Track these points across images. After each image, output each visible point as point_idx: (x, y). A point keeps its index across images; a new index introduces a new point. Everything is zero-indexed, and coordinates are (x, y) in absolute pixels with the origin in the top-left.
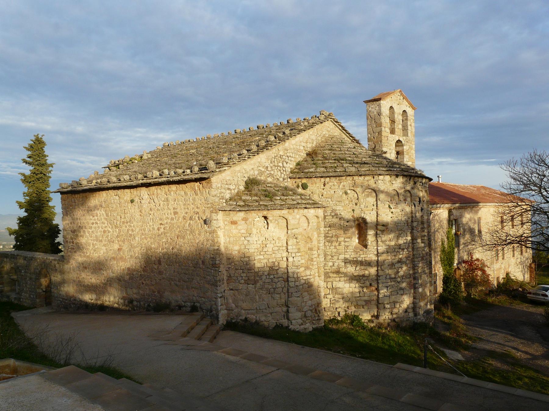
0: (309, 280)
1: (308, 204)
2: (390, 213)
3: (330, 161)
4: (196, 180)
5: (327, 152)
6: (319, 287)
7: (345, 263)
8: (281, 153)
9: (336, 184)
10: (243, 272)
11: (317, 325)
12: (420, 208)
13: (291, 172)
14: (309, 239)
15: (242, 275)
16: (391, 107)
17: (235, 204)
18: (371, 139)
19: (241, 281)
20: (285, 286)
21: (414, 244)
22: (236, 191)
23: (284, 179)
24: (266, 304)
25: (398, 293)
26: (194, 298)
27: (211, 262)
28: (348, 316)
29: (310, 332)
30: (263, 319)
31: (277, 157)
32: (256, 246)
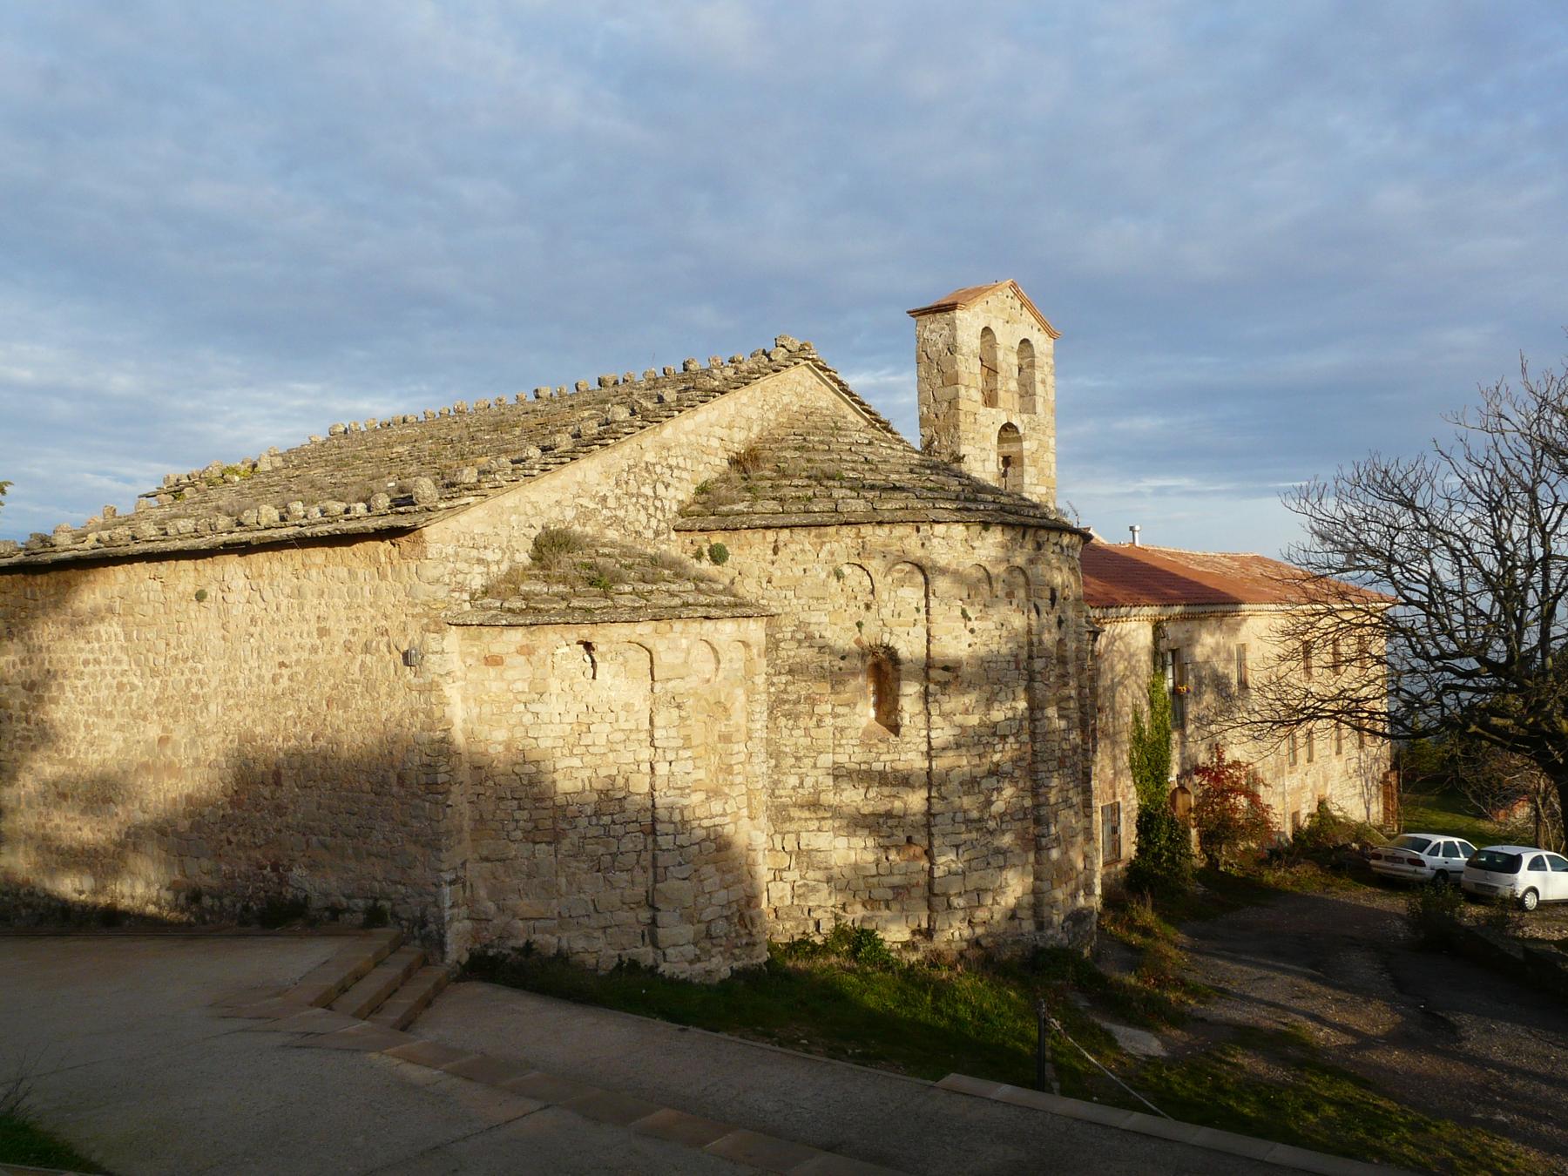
0: (719, 828)
1: (715, 606)
2: (967, 632)
3: (796, 482)
4: (380, 535)
5: (789, 454)
6: (750, 848)
7: (836, 777)
8: (650, 457)
9: (808, 547)
10: (520, 808)
11: (745, 962)
12: (1053, 619)
13: (682, 513)
14: (720, 710)
15: (517, 815)
16: (987, 330)
17: (499, 604)
18: (928, 419)
19: (513, 833)
20: (645, 847)
21: (1037, 723)
22: (505, 567)
23: (657, 534)
24: (590, 902)
25: (988, 864)
26: (376, 884)
27: (423, 779)
28: (844, 932)
29: (722, 981)
30: (579, 945)
31: (637, 470)
32: (556, 730)
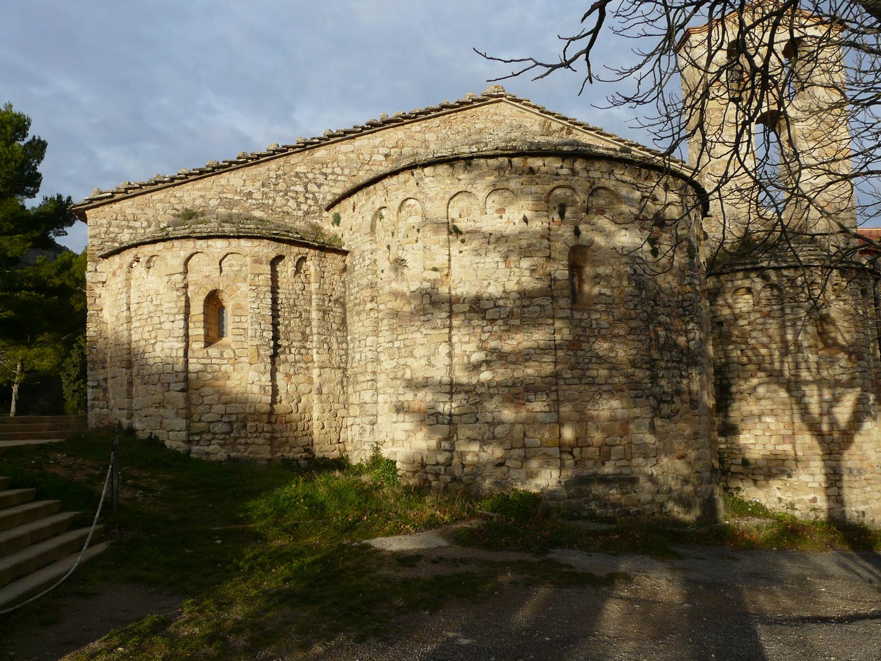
2: (459, 242)
25: (478, 420)
